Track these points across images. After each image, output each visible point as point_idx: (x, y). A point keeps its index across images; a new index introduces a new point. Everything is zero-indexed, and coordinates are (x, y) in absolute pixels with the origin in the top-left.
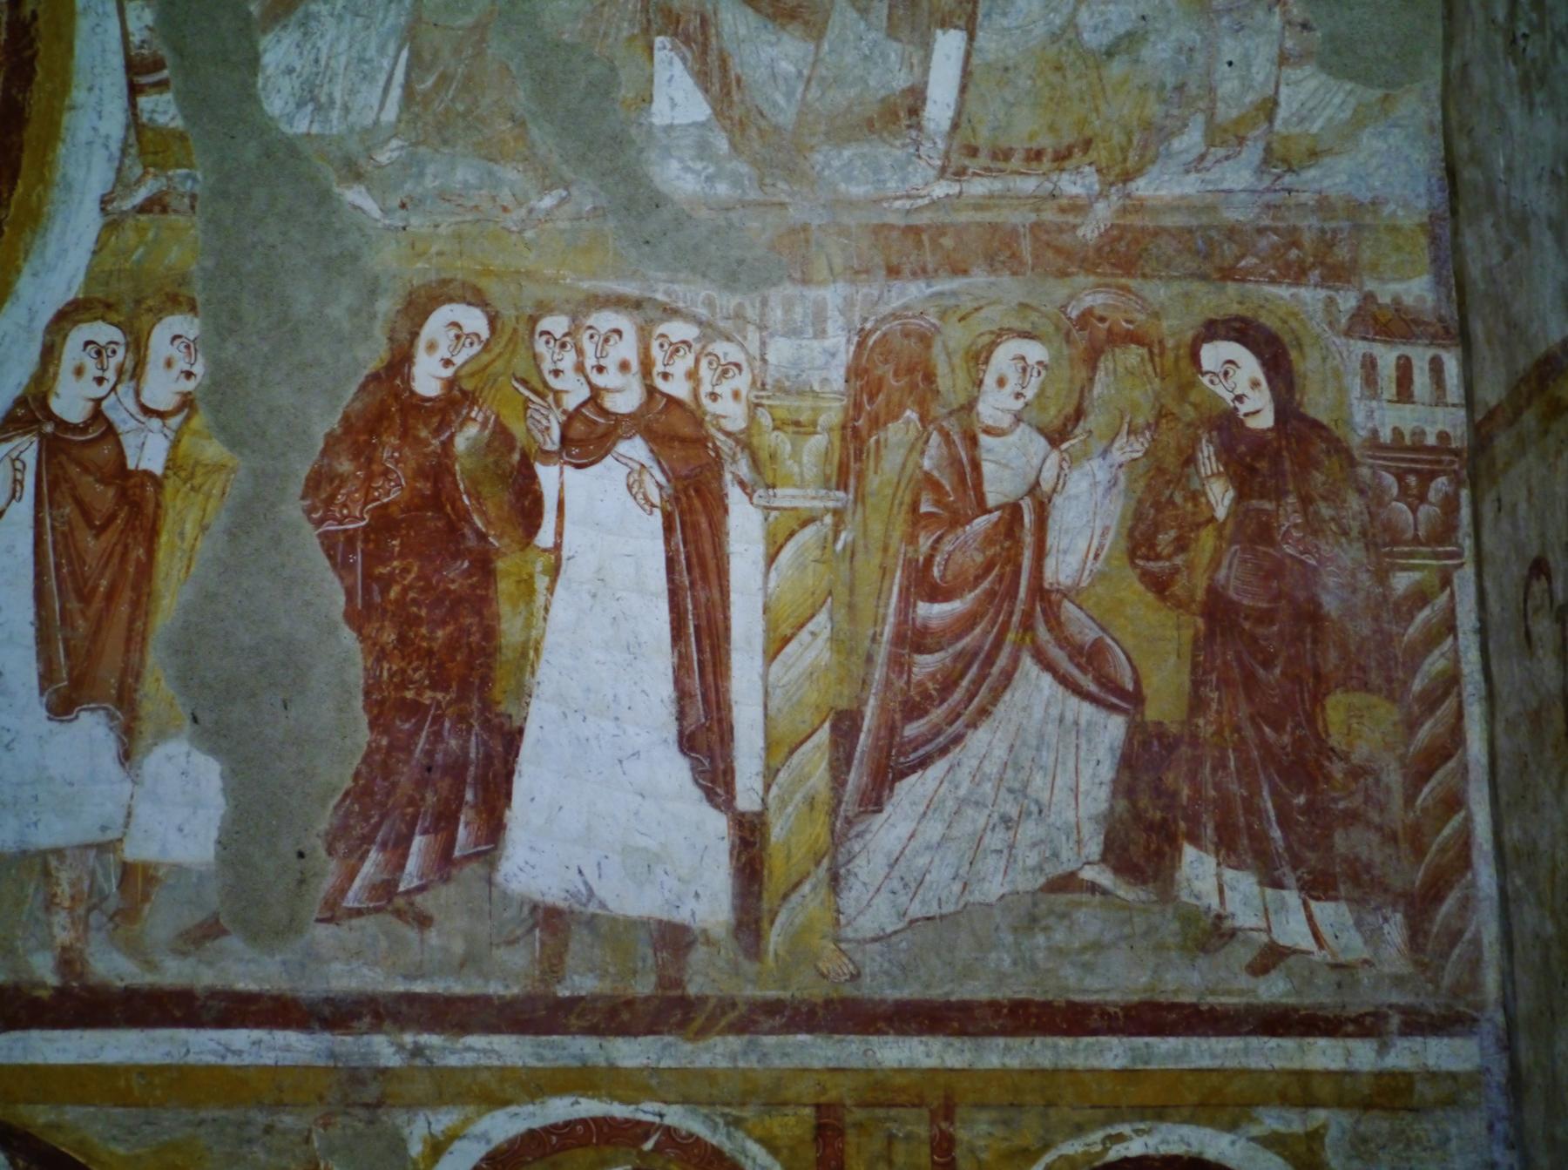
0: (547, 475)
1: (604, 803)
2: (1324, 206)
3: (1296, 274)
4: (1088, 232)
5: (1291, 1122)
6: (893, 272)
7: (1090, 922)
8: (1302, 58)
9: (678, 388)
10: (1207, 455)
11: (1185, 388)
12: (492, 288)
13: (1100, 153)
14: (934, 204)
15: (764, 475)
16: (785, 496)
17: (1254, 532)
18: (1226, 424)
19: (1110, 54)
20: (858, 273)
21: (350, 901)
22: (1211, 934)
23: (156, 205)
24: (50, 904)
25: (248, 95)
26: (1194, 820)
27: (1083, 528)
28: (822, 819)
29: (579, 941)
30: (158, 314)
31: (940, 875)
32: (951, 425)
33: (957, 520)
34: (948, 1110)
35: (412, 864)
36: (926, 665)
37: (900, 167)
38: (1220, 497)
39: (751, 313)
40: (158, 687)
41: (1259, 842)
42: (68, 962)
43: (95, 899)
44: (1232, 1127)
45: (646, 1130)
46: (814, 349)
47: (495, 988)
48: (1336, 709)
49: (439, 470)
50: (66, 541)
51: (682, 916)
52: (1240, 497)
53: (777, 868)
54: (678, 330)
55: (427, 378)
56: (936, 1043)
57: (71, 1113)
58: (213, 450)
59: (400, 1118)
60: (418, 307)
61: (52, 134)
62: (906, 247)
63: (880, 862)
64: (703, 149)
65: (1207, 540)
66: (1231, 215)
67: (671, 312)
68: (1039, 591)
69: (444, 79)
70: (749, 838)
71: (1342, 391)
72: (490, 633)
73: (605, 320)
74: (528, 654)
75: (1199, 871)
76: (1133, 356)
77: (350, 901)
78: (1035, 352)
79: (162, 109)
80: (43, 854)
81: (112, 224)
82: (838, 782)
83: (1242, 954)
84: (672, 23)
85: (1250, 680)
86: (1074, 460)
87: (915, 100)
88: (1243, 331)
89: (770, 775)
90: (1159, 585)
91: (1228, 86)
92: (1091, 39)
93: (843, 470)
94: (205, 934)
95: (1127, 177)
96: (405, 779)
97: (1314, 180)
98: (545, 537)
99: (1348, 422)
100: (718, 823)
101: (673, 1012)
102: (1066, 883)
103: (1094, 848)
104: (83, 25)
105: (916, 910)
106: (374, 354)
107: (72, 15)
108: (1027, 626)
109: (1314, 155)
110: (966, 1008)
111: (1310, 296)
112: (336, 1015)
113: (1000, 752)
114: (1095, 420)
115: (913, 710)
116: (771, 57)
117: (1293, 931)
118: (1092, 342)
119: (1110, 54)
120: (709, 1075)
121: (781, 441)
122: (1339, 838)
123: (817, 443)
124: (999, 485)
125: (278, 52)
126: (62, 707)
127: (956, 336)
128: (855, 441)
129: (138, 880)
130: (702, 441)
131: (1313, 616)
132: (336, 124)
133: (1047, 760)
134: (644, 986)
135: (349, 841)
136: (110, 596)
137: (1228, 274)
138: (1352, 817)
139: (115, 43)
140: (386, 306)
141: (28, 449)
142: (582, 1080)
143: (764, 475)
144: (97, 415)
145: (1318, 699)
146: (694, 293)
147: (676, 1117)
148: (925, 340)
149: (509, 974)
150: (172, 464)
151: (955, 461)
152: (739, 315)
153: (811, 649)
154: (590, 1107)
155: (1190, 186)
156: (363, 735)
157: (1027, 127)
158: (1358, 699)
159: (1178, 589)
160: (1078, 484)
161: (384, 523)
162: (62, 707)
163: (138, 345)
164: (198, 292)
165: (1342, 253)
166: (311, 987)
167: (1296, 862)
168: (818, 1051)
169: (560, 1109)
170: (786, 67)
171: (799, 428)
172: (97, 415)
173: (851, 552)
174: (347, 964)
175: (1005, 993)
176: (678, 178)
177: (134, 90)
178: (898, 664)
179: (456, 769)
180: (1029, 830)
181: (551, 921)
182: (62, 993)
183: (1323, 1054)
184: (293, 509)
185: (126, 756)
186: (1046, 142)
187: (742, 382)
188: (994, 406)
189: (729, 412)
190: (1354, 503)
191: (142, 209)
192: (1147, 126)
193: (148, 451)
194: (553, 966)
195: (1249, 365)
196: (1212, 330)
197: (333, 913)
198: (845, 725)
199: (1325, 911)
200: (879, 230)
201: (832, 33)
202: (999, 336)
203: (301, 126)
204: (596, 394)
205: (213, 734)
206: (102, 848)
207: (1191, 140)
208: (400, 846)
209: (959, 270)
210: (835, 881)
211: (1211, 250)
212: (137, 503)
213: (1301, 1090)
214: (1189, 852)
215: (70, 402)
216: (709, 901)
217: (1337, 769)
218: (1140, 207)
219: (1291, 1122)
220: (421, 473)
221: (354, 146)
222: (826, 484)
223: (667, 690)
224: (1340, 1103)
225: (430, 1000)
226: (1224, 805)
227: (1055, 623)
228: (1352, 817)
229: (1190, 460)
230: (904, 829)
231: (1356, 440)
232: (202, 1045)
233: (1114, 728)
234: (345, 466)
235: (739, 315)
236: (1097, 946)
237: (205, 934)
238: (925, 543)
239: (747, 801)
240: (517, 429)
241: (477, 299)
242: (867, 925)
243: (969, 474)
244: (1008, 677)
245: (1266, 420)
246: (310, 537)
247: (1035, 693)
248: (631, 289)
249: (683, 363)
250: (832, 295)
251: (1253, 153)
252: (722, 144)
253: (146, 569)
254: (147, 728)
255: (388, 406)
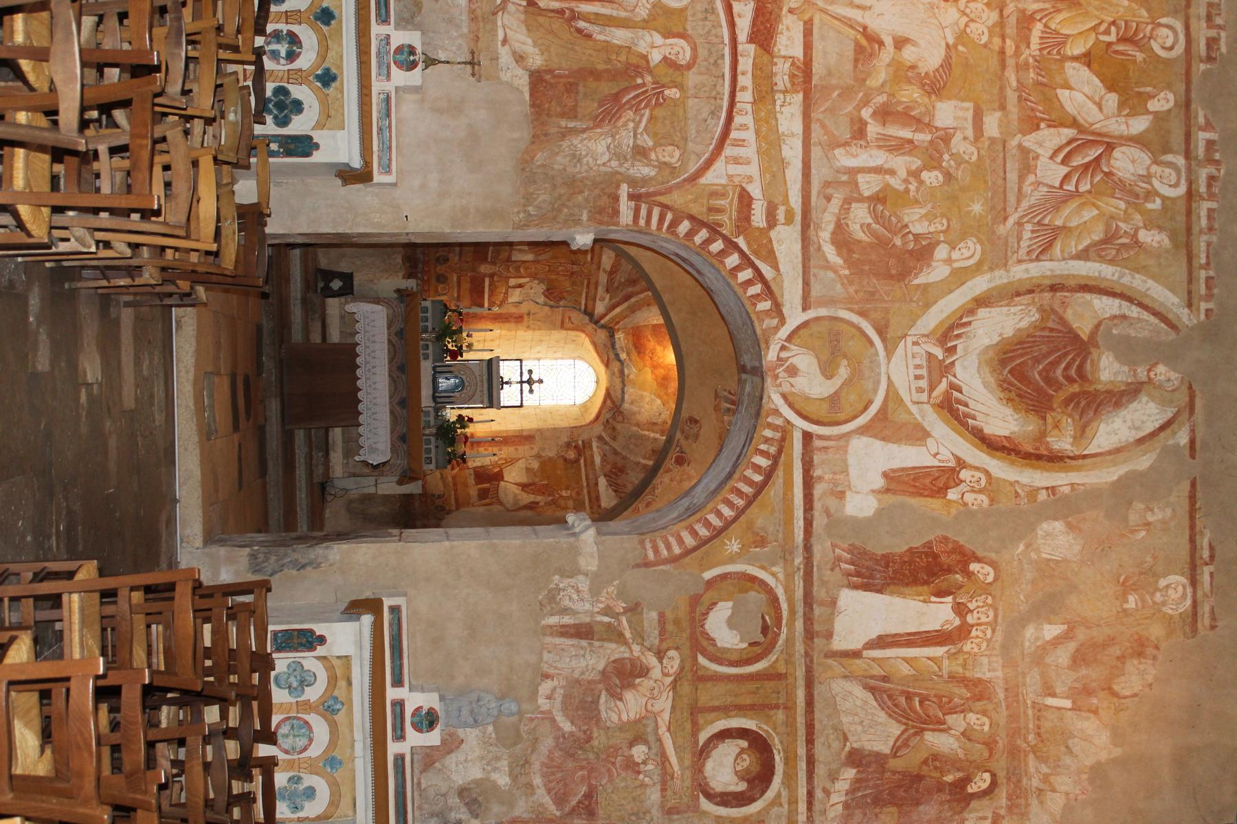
0: (949, 599)
1: (863, 616)
2: (1027, 805)
3: (1009, 798)
4: (1019, 742)
5: (784, 800)
6: (1006, 690)
7: (836, 745)
8: (1068, 799)
9: (974, 633)
10: (960, 775)
11: (978, 768)
12: (999, 584)
13: (1040, 745)
14: (1025, 701)
15: (952, 656)
16: (946, 663)
17: (940, 787)
18: (967, 780)
19: (1067, 747)
20: (1006, 681)
21: (837, 551)
22: (833, 777)
23: (1017, 495)
24: (835, 473)
25: (1047, 518)
26: (863, 772)
27: (942, 742)
28: (861, 673)
29: (830, 611)
30: (989, 496)
31: (848, 705)
32: (966, 706)
33: (941, 707)
34: (786, 708)
35: (847, 566)
36: (902, 700)
37: (1035, 691)
38: (949, 778)
39: (995, 652)
40: (891, 499)
41: (858, 789)
42: (820, 478)
43: (836, 485)
44: (783, 783)
45: (780, 629)
46: (985, 668)
47: (815, 588)
48: (893, 809)
49: (949, 570)
50: (928, 474)
51: (835, 637)
52: (950, 784)
53: (845, 661)
54: (989, 633)
55: (974, 567)
56: (803, 704)
57: (781, 480)
58: (953, 511)
59: (782, 565)
60: (992, 564)
61: (1033, 467)
62: (1013, 691)
63: (850, 689)
64: (1037, 639)
65: (936, 774)
66: (1024, 781)
67: (994, 631)
68: (923, 730)
69: (1053, 570)
70: (856, 654)
71: (978, 811)
72: (907, 585)
73: (991, 613)
74: (904, 595)
75: (850, 773)
76: (986, 754)
77: (837, 551)
78: (986, 728)
79: (1043, 495)
80: (847, 471)
81: (1011, 484)
82: (872, 677)
83: (828, 785)
84: (1071, 629)
85: (899, 787)
86: (958, 739)
87: (1054, 695)
88: (994, 783)
89: (873, 660)
90: (925, 762)
91: (1059, 778)
92: (1070, 743)
93: (953, 677)
94: (827, 513)
95: (1034, 753)
96: (870, 563)
97: (1034, 802)
98: (933, 599)
99: (970, 812)
100: (859, 646)
101: (810, 635)
102: (846, 739)
103: (855, 745)
104: (1063, 475)
105: (838, 699)
106: (980, 553)
107: (1067, 472)
108: (913, 727)
109: (1041, 802)
110: (813, 712)
111: (1004, 802)
112: (808, 548)
113: (879, 720)
114: (969, 745)
115: (890, 697)
116: (1063, 656)
117: (835, 798)
118: (990, 744)
119: (1067, 747)
120: (793, 645)
121: (960, 661)
122: (857, 811)
123: (961, 670)
124: (950, 719)
125: (1058, 525)
126: (885, 475)
127: (990, 707)
128: (963, 681)
129: (841, 495)
130: (960, 640)
131: (918, 804)
132: (1040, 541)
133: (878, 732)
134: (817, 627)
135: (852, 549)
136: (915, 486)
137: (1009, 779)
138: (865, 814)
139: (1059, 483)
140: (993, 556)
141: (952, 464)
142: (792, 612)
143: (952, 656)
144: (962, 481)
145: (896, 805)
146: (999, 636)
147: (783, 636)
148: (988, 699)
149: (819, 592)
150: (950, 501)
151: (956, 707)
152: (994, 649)
153: (906, 670)
154: (785, 614)
155: (1032, 770)
156: (880, 552)
157: (1047, 725)
158: (896, 815)
159: (925, 768)
160: (951, 740)
161: (936, 556)
162: (885, 475)
163: (980, 491)
164: (995, 506)
165: (1015, 811)
166: (814, 540)
167: (853, 800)
168: (800, 673)
169: (784, 606)
170: (1060, 660)
171: (964, 666)
172: (962, 481)
173: (931, 679)
174: (820, 550)
175: (816, 722)
176: (1030, 632)
177: (1047, 488)
178: (903, 692)
179: (871, 577)
180: (859, 728)
181: (833, 603)
182: (812, 477)
183: (802, 807)
184: (939, 532)
185: (873, 491)
186: (1043, 730)
187: (976, 650)
188: (972, 717)
189: (967, 647)
190: (949, 814)
191: (1016, 492)
192: (1048, 757)
193: (952, 495)
194: (822, 604)
195: (985, 786)
196: (994, 776)
197: (834, 546)
198: (885, 679)
199: (840, 807)
200: (1018, 686)
201: (1070, 672)
202: (990, 718)
203: (1040, 532)
204: (972, 611)
205: (879, 513)
206: (849, 486)
207: (1045, 769)
208: (852, 563)
209: (1008, 707)
210: (846, 677)
211: (1016, 776)
212: (941, 492)
213: (793, 801)
214: (854, 771)
215: (964, 474)
216: (838, 644)
217: (877, 810)
218: (1026, 756)
219: (784, 800)
220: (949, 566)
221: (1035, 546)
222: (950, 672)
223: (894, 632)
224: (790, 811)
225: (812, 571)
226: (866, 780)
227: (916, 734)
228: (865, 814)
229: (959, 770)
230: (859, 695)
231: (965, 815)
232: (799, 513)
233: (886, 750)
234: (950, 546)
235: (994, 649)
236: (829, 746)
237: (827, 513)
238: (935, 700)
239: (866, 653)
240: (962, 591)
241: (996, 579)
242: (834, 686)
243: (952, 711)
244: (899, 722)
245: (970, 790)
246: (932, 537)
247: (896, 729)
248: (999, 620)
249: (979, 634)
250: (1000, 674)
251: (1042, 786)
252: (1039, 644)
253: (921, 495)
254: (880, 496)
255: (965, 558)
